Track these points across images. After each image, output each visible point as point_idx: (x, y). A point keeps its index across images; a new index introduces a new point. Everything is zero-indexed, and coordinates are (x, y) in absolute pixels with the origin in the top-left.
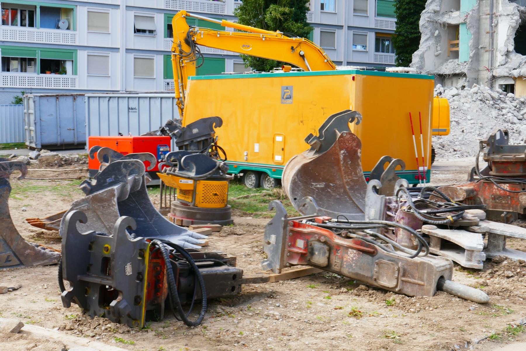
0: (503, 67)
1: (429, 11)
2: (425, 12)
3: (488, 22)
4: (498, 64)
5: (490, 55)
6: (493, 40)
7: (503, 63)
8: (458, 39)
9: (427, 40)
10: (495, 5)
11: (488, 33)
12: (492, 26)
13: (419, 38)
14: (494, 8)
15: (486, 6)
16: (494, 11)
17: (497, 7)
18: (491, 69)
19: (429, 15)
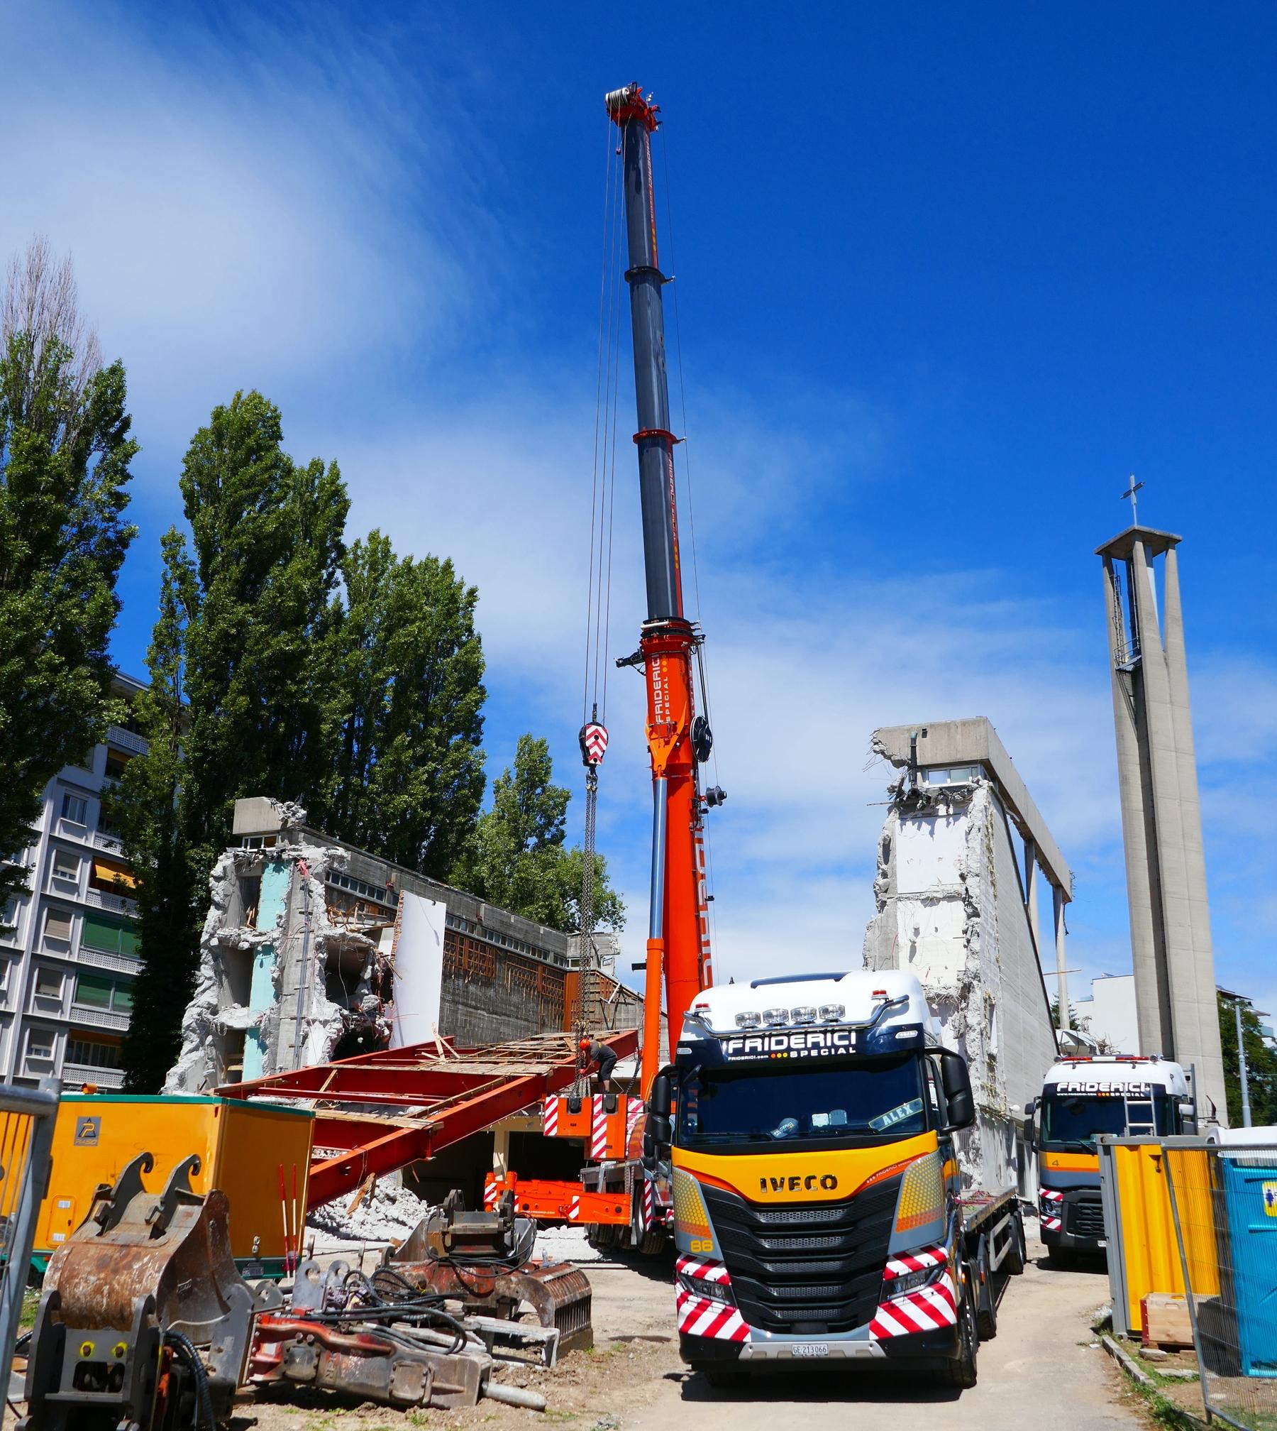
1: (199, 1004)
8: (242, 1052)
9: (191, 1051)
10: (305, 1004)
13: (180, 1046)
14: (305, 1008)
15: (292, 1005)
16: (304, 1013)
17: (309, 1008)
19: (199, 1010)
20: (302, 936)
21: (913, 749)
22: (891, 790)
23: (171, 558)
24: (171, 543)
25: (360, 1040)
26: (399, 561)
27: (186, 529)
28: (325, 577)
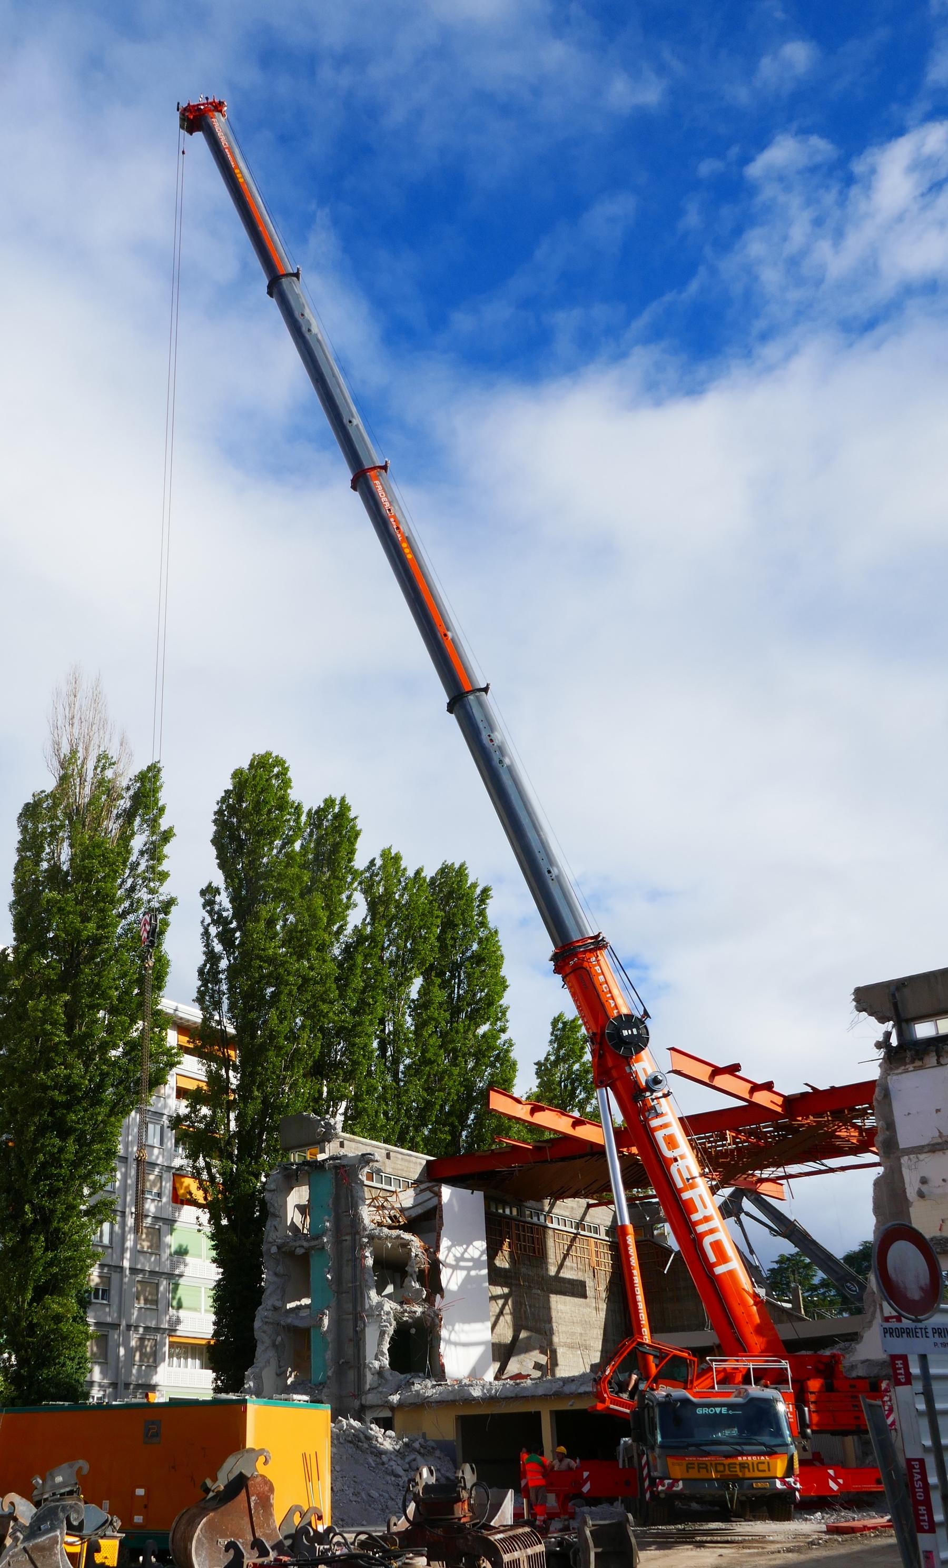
0: (375, 1391)
2: (263, 1309)
3: (350, 1325)
4: (368, 1387)
5: (356, 1373)
6: (359, 1350)
7: (375, 1385)
11: (351, 1340)
12: (356, 1331)
14: (359, 1305)
16: (359, 1309)
18: (358, 1395)
20: (348, 1238)
21: (895, 1005)
22: (879, 1045)
23: (209, 904)
24: (209, 892)
25: (413, 1331)
26: (411, 873)
27: (219, 880)
28: (345, 900)
